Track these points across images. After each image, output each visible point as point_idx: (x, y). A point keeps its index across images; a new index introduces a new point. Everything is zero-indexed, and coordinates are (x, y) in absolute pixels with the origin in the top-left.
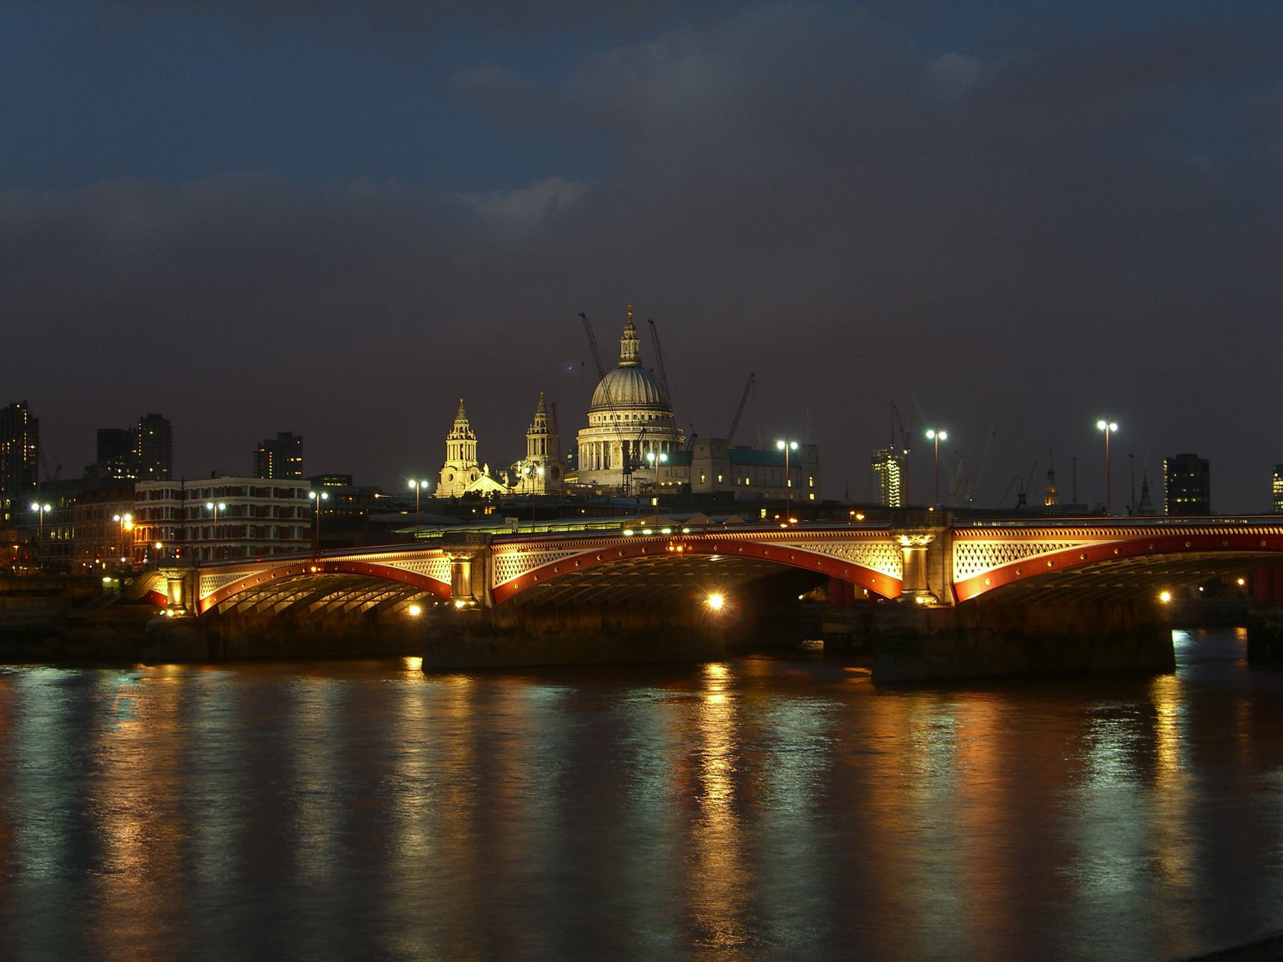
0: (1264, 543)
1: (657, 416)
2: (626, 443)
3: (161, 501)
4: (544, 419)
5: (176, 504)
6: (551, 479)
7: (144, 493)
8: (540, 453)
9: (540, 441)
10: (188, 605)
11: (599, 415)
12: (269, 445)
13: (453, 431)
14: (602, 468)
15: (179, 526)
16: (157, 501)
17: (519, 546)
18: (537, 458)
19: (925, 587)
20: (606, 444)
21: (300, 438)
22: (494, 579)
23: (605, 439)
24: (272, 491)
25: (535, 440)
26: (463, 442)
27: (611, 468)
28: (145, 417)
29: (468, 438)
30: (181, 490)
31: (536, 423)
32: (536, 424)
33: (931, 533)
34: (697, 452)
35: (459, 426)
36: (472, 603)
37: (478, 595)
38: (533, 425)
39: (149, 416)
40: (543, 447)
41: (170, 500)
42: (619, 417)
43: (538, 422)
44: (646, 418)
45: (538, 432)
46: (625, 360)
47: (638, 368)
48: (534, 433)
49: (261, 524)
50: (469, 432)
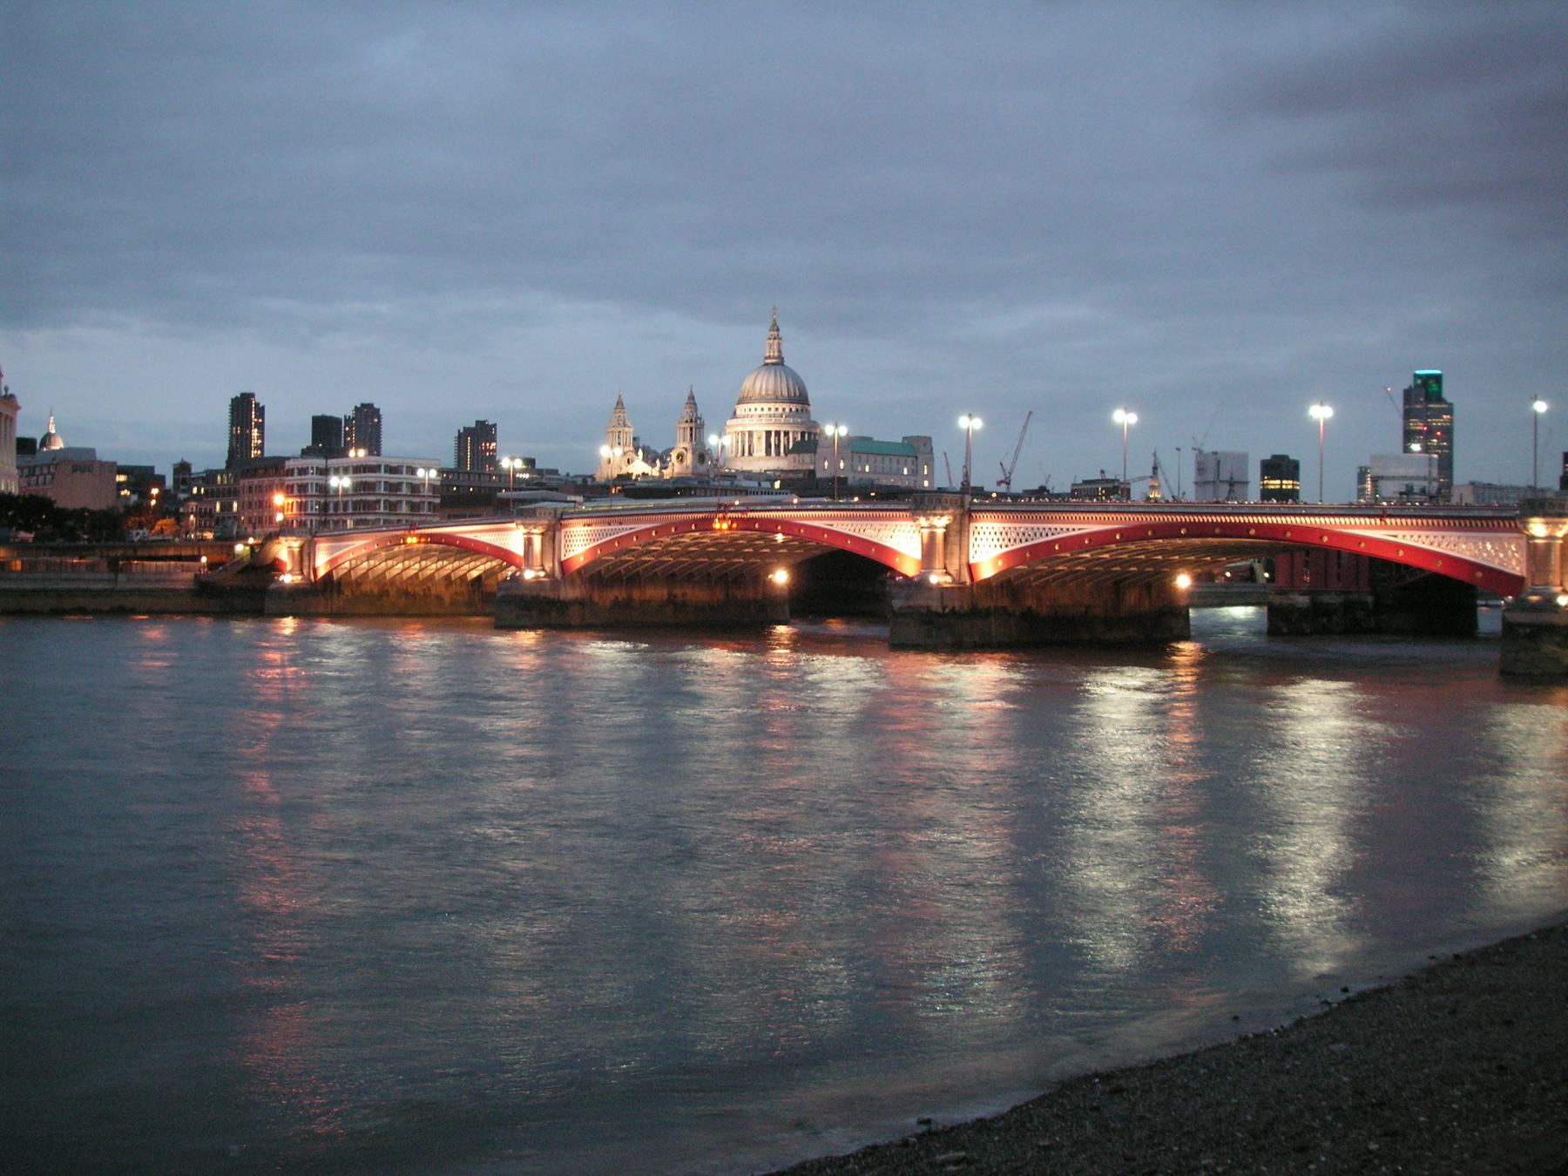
0: (1252, 532)
2: (768, 433)
3: (307, 477)
7: (293, 470)
10: (305, 571)
12: (468, 432)
14: (746, 454)
16: (303, 477)
17: (585, 521)
19: (942, 566)
20: (751, 434)
21: (495, 425)
22: (563, 552)
23: (750, 429)
27: (754, 455)
28: (359, 406)
33: (949, 514)
36: (542, 574)
37: (548, 566)
39: (363, 405)
40: (691, 435)
41: (315, 476)
44: (787, 410)
49: (393, 499)
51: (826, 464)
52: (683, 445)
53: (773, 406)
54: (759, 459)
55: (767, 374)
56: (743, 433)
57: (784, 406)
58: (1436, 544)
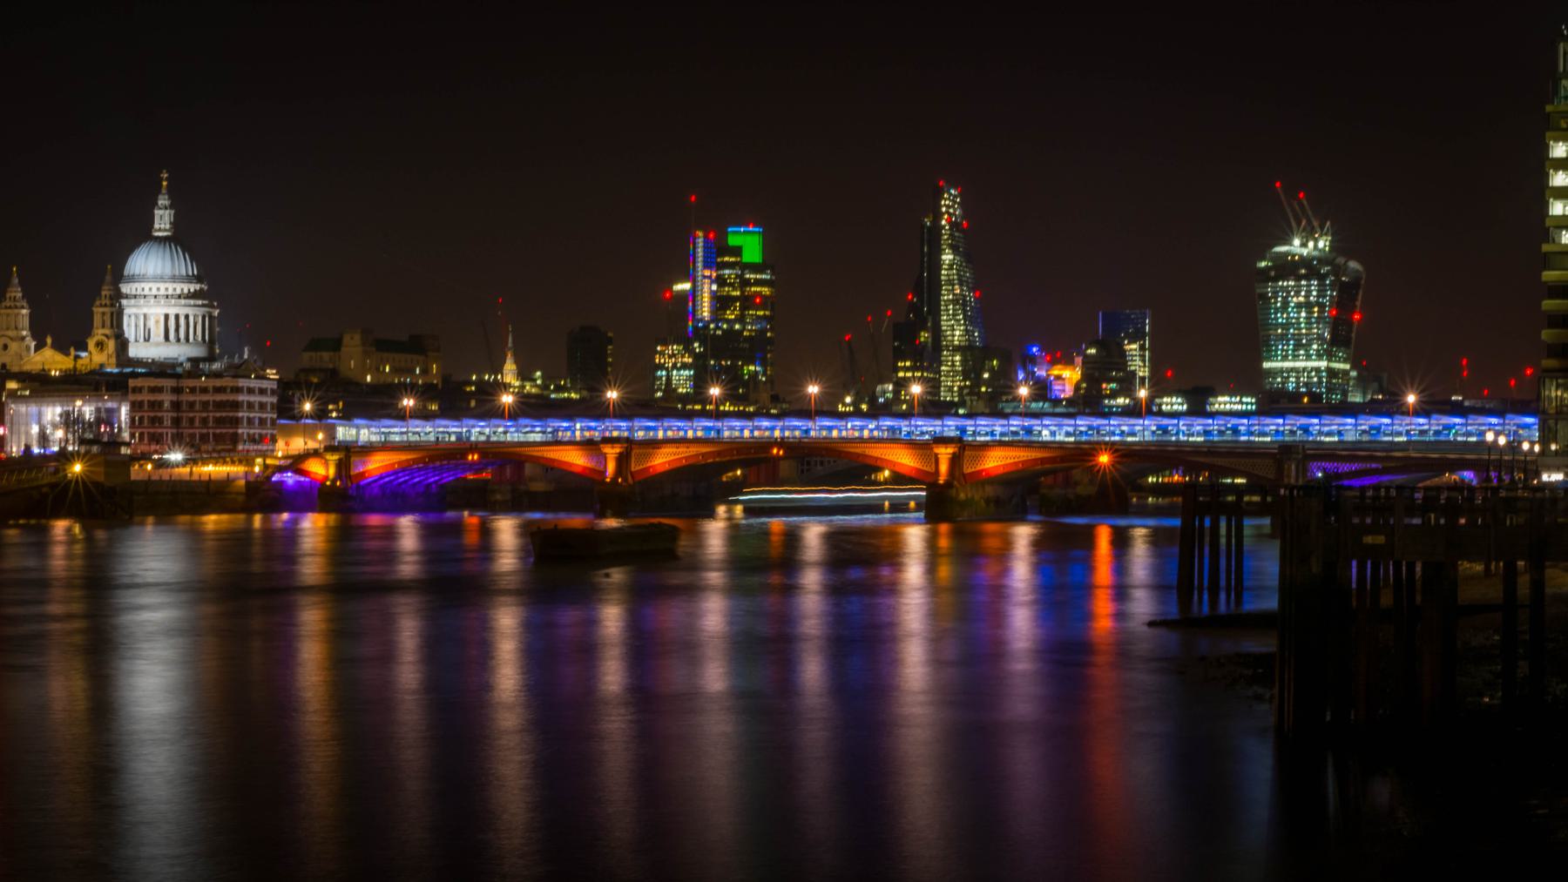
1: (195, 290)
2: (167, 317)
4: (112, 293)
5: (174, 398)
9: (109, 315)
13: (5, 300)
15: (175, 415)
18: (107, 331)
24: (257, 391)
25: (104, 314)
32: (103, 297)
34: (346, 339)
35: (13, 294)
38: (100, 299)
42: (158, 289)
43: (106, 296)
44: (186, 291)
45: (106, 305)
46: (160, 230)
47: (179, 239)
48: (101, 306)
51: (352, 362)
52: (101, 331)
53: (171, 286)
55: (161, 254)
56: (137, 316)
57: (183, 285)
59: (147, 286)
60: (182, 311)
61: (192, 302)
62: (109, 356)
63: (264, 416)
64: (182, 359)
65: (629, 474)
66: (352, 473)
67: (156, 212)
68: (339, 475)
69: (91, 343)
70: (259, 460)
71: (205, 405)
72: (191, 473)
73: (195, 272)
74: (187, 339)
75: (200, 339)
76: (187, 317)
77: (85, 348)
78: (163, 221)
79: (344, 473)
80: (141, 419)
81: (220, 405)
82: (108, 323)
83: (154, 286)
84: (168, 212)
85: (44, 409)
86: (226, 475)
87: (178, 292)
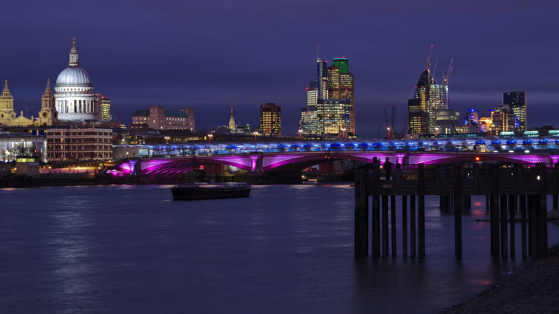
1: (88, 89)
2: (75, 101)
5: (66, 137)
6: (54, 118)
8: (49, 106)
9: (49, 101)
11: (62, 88)
13: (2, 95)
15: (67, 145)
22: (264, 164)
25: (46, 100)
26: (7, 100)
27: (69, 112)
29: (10, 98)
30: (67, 132)
31: (46, 93)
32: (46, 94)
34: (152, 110)
35: (5, 93)
42: (72, 89)
44: (84, 90)
45: (47, 97)
46: (72, 63)
47: (81, 66)
48: (45, 97)
50: (10, 95)
51: (154, 121)
52: (45, 108)
54: (71, 114)
56: (62, 101)
57: (82, 88)
58: (530, 160)
59: (66, 88)
60: (82, 99)
61: (87, 95)
62: (49, 119)
63: (107, 145)
64: (82, 120)
65: (262, 168)
66: (142, 169)
67: (70, 55)
68: (135, 169)
69: (41, 114)
70: (101, 164)
71: (80, 140)
72: (70, 170)
73: (88, 82)
74: (85, 111)
75: (90, 111)
76: (84, 101)
77: (38, 116)
78: (73, 58)
79: (138, 169)
80: (53, 146)
81: (86, 140)
82: (48, 105)
83: (70, 88)
84: (75, 55)
85: (10, 143)
86: (86, 171)
87: (81, 90)
